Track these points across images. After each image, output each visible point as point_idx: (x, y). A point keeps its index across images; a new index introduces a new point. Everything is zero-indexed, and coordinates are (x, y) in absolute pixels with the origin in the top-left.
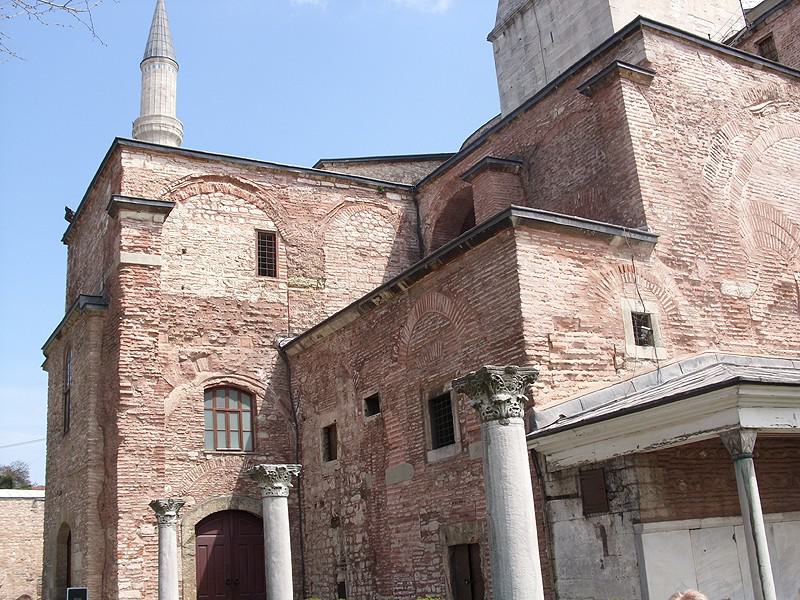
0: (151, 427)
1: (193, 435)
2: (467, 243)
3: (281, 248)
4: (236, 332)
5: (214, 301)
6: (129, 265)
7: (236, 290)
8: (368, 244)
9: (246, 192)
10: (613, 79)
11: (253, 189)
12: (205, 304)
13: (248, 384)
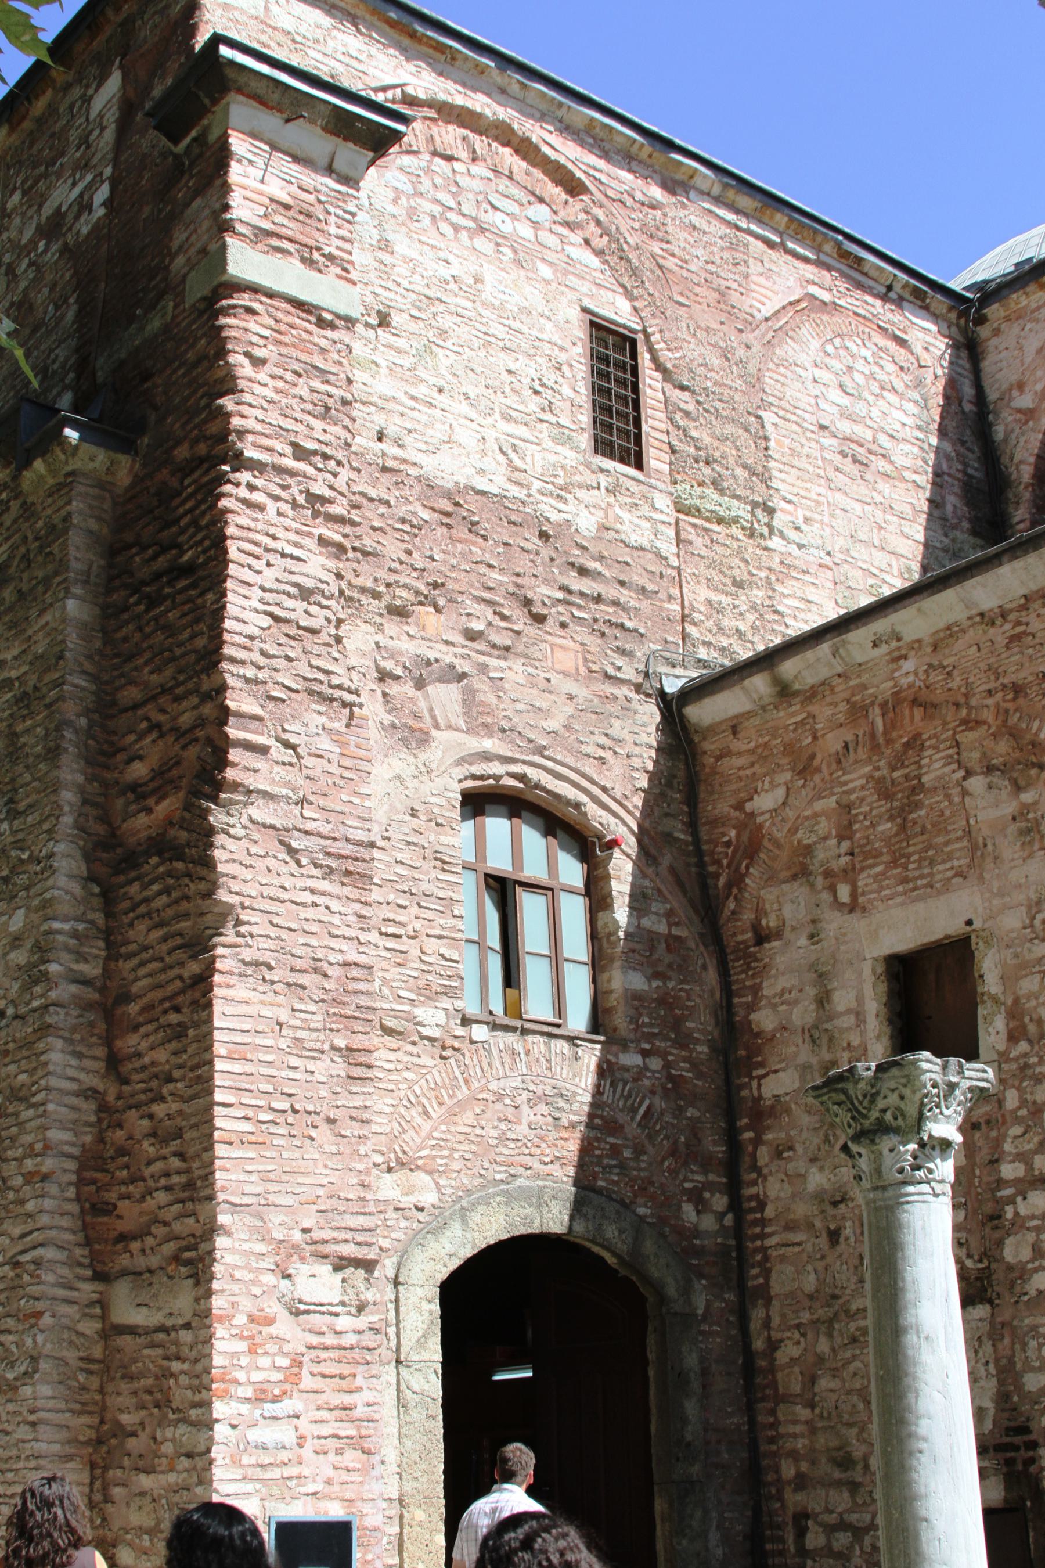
0: (324, 885)
1: (432, 945)
4: (539, 619)
5: (471, 497)
6: (254, 289)
7: (537, 485)
8: (868, 435)
11: (574, 187)
12: (449, 508)
13: (583, 798)
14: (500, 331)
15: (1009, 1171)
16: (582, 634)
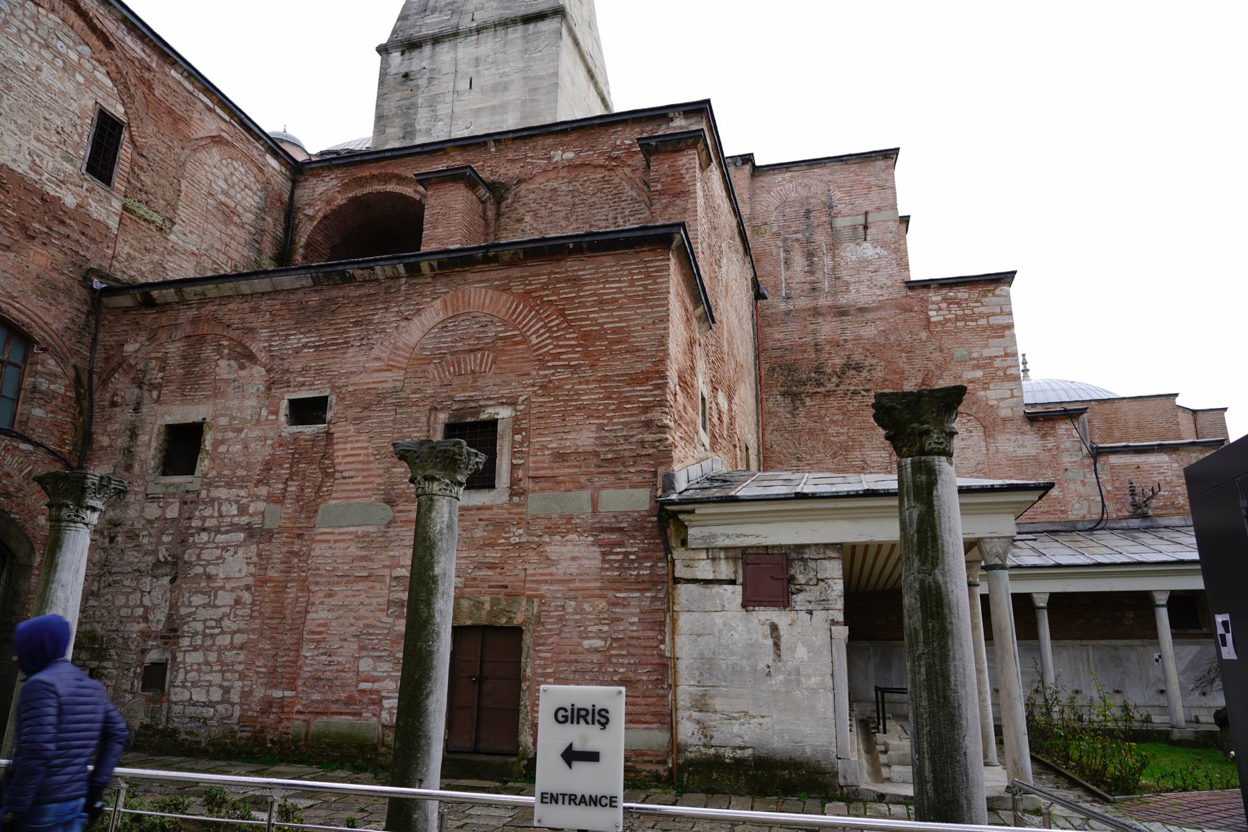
2: (584, 245)
3: (125, 152)
7: (46, 175)
8: (233, 205)
9: (94, 40)
10: (688, 147)
11: (109, 45)
14: (45, 97)
15: (196, 523)
16: (54, 251)
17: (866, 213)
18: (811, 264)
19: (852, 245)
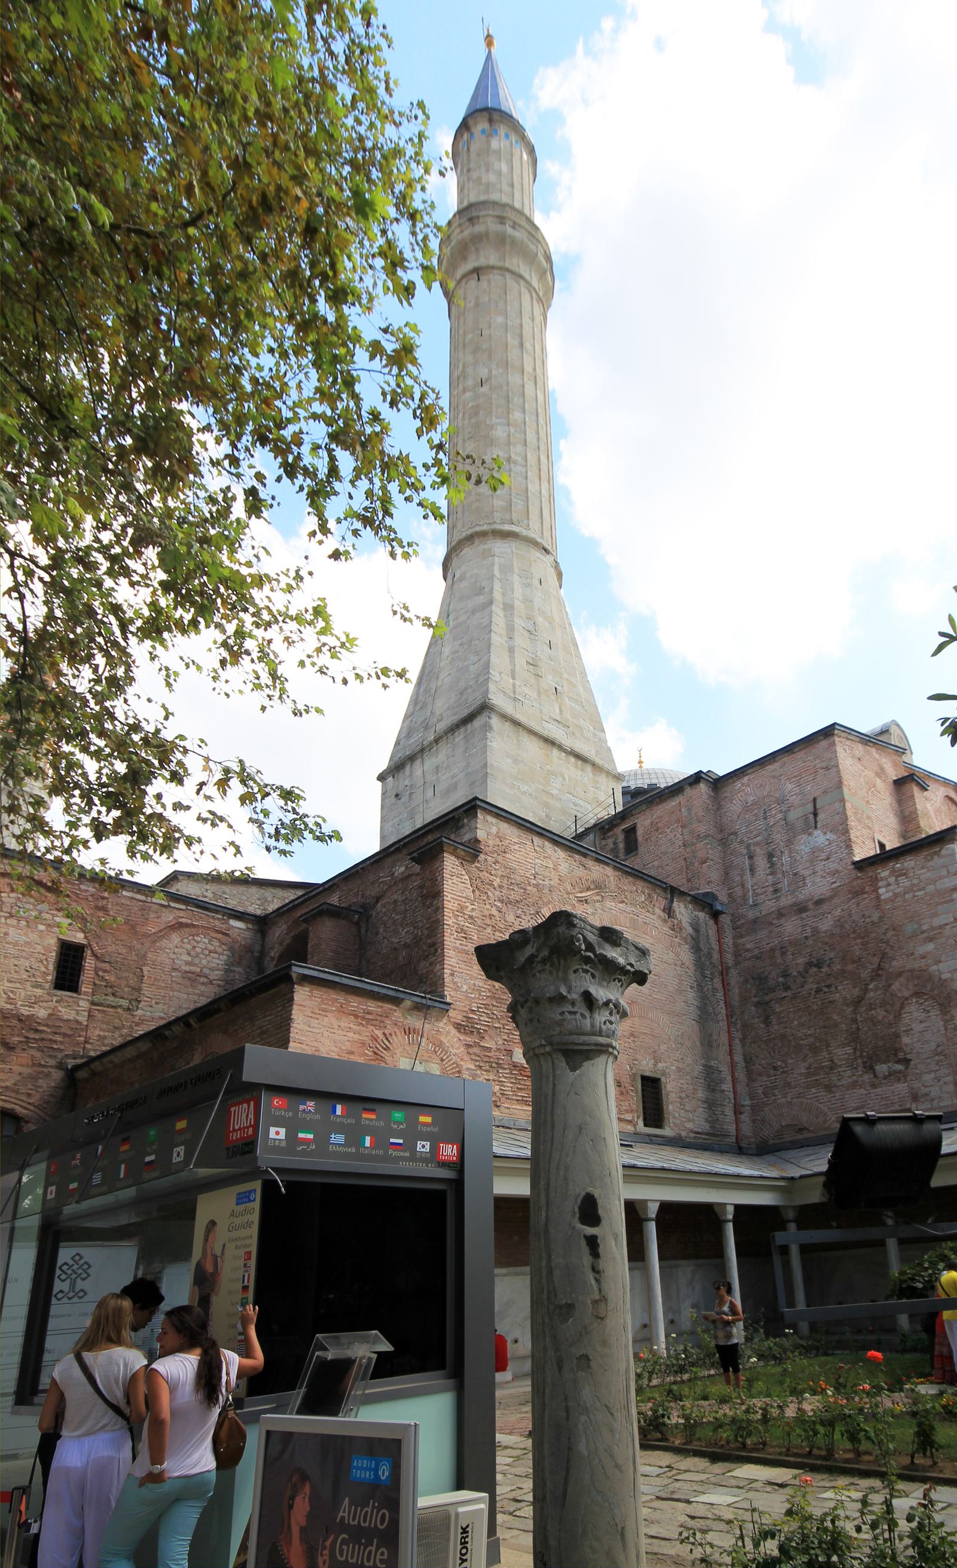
17: (815, 799)
18: (772, 865)
19: (805, 837)
